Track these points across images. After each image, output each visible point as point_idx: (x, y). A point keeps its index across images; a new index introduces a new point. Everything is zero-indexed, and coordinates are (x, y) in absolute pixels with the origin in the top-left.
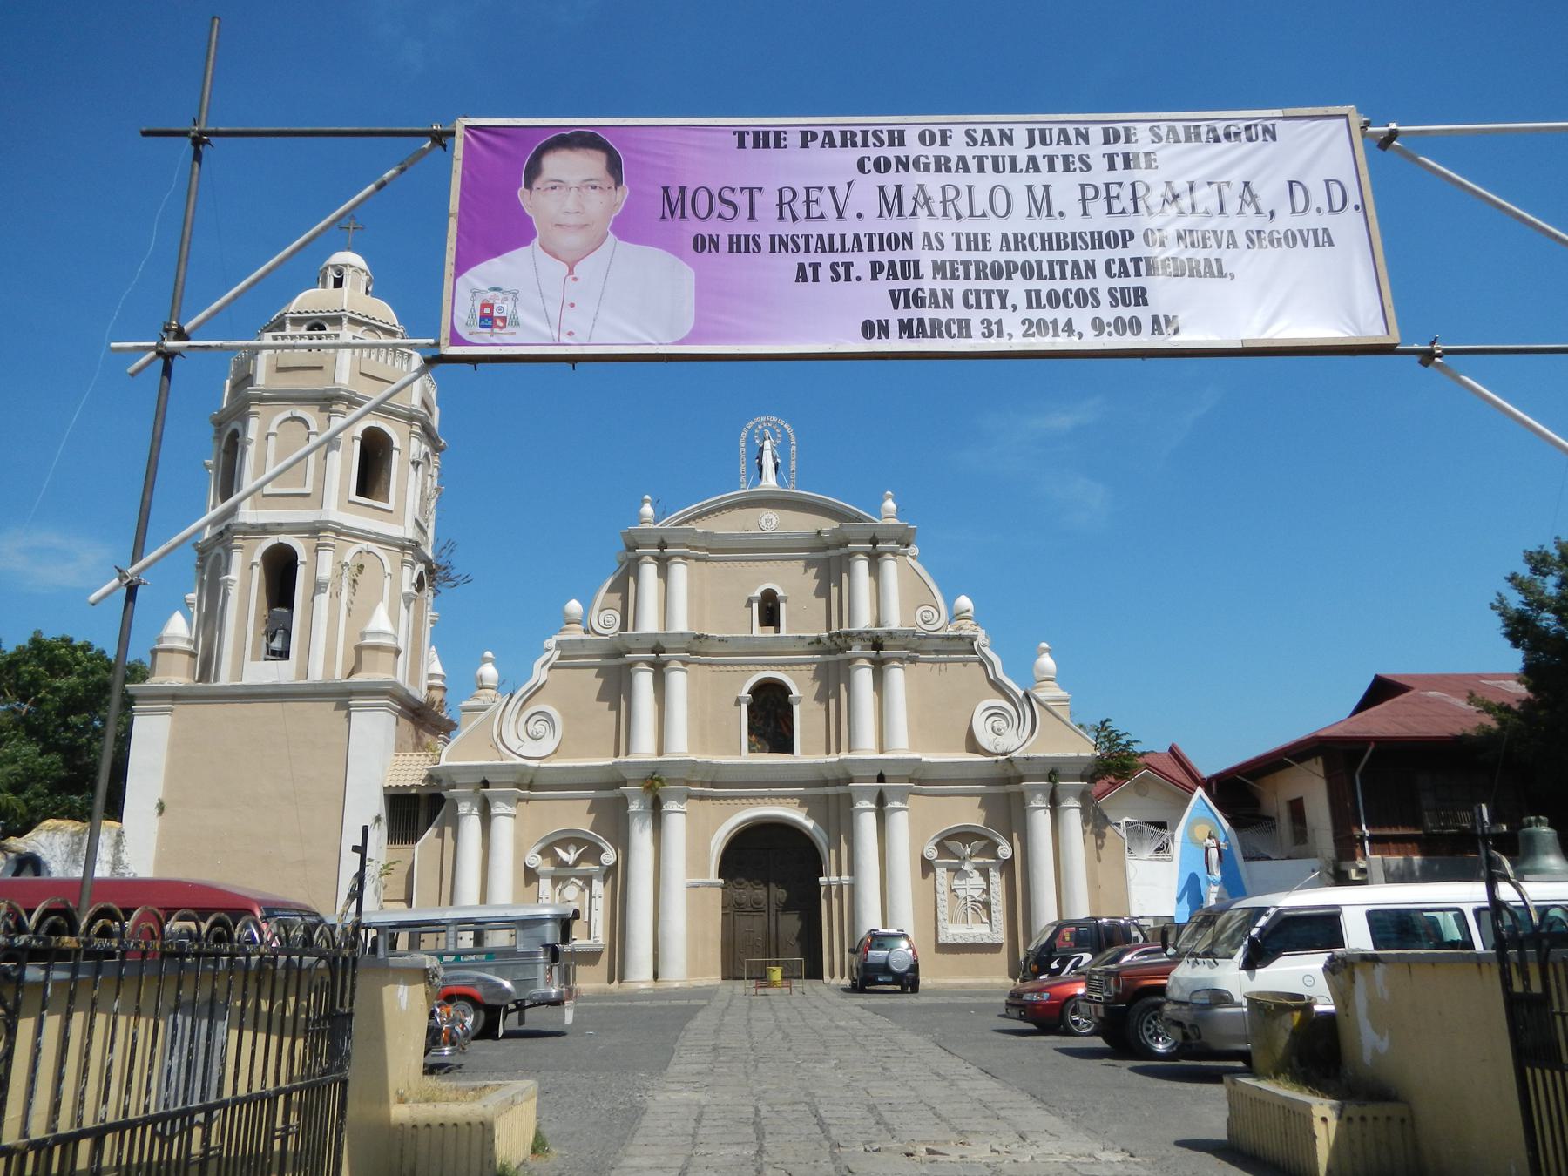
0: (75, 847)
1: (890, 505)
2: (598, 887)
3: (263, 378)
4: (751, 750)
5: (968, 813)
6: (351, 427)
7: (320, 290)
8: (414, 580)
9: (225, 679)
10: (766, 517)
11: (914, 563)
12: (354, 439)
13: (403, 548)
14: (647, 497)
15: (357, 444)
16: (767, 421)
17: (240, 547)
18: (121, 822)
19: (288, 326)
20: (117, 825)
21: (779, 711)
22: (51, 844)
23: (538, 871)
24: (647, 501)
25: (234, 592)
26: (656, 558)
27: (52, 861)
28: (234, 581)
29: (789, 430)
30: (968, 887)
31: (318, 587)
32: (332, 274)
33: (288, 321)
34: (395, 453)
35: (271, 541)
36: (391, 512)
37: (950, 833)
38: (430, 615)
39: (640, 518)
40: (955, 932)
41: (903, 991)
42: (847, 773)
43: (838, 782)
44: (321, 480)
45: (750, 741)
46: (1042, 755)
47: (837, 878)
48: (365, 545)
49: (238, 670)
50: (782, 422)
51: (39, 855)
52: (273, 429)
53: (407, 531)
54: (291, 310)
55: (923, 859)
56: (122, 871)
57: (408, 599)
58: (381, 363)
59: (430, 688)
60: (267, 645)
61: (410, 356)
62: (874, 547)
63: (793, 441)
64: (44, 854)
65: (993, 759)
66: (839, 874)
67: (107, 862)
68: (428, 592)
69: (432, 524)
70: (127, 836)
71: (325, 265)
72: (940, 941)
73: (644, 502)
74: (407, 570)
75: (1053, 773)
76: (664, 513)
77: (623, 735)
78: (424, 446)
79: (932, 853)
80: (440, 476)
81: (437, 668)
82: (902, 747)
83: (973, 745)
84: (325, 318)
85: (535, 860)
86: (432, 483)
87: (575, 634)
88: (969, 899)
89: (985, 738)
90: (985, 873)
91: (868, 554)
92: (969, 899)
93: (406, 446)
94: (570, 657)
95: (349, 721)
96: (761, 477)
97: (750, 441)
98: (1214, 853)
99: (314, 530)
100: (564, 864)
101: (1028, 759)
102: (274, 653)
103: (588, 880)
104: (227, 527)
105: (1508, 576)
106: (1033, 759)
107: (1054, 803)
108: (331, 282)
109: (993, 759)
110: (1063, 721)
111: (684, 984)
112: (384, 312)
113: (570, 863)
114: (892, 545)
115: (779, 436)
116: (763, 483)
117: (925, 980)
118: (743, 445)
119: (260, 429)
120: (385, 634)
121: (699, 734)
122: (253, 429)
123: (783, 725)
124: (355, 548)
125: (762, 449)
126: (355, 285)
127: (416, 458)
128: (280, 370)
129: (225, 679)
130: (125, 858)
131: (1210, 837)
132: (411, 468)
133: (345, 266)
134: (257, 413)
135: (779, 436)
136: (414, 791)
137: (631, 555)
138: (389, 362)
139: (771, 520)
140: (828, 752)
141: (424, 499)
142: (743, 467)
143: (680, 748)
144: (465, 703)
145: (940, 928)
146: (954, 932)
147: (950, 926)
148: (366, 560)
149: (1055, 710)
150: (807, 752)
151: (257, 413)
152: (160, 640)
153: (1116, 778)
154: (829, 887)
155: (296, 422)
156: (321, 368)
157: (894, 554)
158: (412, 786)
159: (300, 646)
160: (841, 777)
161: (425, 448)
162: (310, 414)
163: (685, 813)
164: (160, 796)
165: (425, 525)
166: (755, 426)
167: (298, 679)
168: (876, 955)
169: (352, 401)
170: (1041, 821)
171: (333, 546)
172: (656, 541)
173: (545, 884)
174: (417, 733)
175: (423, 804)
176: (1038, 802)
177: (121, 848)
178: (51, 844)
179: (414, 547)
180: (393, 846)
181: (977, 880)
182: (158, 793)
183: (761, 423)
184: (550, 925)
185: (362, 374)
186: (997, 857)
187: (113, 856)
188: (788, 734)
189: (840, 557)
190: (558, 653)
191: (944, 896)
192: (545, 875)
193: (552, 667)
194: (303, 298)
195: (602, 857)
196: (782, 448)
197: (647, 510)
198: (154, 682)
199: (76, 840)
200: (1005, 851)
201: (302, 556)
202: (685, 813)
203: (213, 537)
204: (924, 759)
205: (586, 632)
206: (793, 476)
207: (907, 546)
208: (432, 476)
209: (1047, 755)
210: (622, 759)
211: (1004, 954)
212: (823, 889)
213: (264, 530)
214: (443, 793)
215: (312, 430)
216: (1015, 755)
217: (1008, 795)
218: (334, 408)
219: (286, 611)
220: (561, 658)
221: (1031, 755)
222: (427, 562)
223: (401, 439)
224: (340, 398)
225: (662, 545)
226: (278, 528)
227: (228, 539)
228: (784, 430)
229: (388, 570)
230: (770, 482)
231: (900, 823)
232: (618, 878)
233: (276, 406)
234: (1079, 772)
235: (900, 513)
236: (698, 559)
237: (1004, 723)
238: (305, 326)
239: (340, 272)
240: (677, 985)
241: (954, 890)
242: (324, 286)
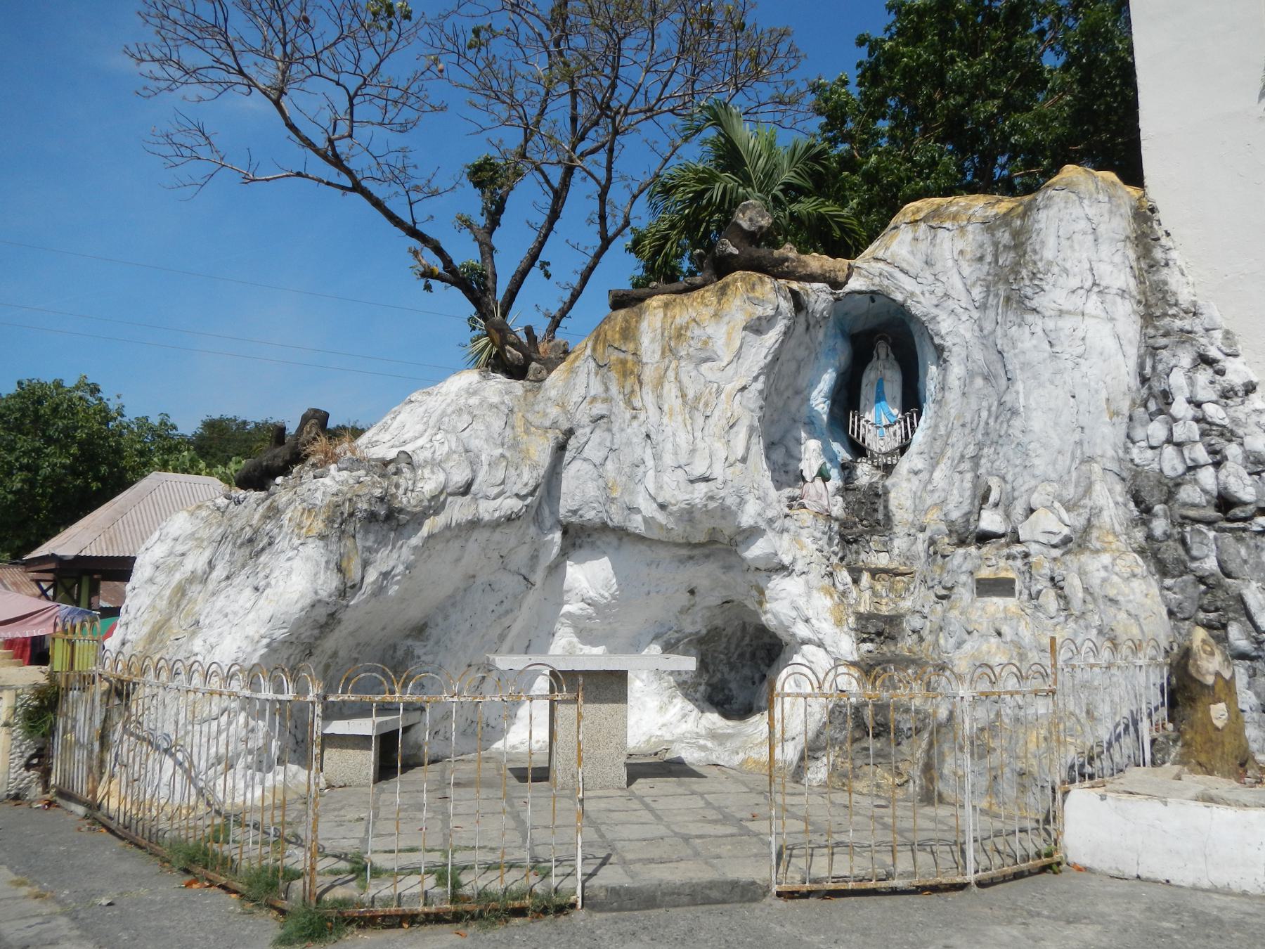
0: (1006, 259)
18: (1132, 174)
27: (942, 315)
51: (899, 297)
56: (1178, 324)
64: (906, 290)
67: (1123, 293)
70: (1167, 218)
130: (1182, 288)
177: (1158, 254)
199: (1005, 237)
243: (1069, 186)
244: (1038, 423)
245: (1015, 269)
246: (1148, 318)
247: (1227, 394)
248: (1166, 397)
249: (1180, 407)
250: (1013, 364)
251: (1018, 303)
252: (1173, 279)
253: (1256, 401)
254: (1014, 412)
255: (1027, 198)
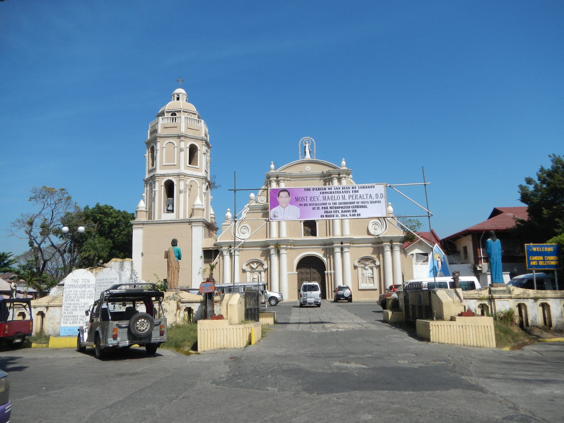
1: (344, 163)
2: (263, 273)
3: (160, 131)
4: (304, 235)
5: (368, 251)
6: (185, 145)
7: (172, 102)
8: (206, 188)
9: (156, 219)
10: (307, 167)
11: (351, 180)
12: (187, 148)
13: (202, 179)
14: (272, 162)
15: (188, 149)
16: (307, 138)
17: (158, 181)
18: (132, 258)
19: (166, 114)
20: (131, 259)
21: (312, 224)
22: (115, 265)
23: (246, 270)
24: (272, 163)
25: (157, 194)
26: (276, 181)
28: (157, 191)
29: (313, 141)
30: (367, 273)
31: (180, 192)
32: (176, 96)
33: (165, 113)
34: (199, 151)
35: (166, 179)
36: (198, 168)
37: (362, 258)
38: (210, 197)
39: (270, 169)
40: (364, 286)
41: (348, 302)
42: (332, 242)
43: (329, 244)
44: (179, 161)
45: (304, 233)
46: (388, 236)
47: (330, 271)
48: (192, 179)
49: (160, 216)
50: (311, 138)
52: (164, 146)
53: (203, 174)
54: (166, 109)
55: (354, 265)
57: (205, 194)
58: (194, 125)
59: (211, 218)
60: (167, 209)
61: (201, 121)
62: (339, 176)
63: (315, 144)
65: (374, 237)
66: (331, 270)
68: (209, 190)
69: (209, 171)
70: (134, 262)
71: (174, 93)
72: (359, 289)
73: (271, 164)
74: (204, 185)
75: (391, 241)
76: (278, 166)
77: (268, 231)
78: (206, 148)
79: (357, 264)
80: (210, 156)
81: (212, 212)
82: (348, 234)
83: (369, 234)
84: (176, 111)
85: (245, 267)
86: (209, 158)
87: (254, 204)
88: (367, 277)
89: (372, 231)
90: (372, 269)
91: (337, 178)
92: (367, 277)
93: (202, 148)
94: (252, 210)
95: (192, 229)
96: (305, 155)
97: (302, 144)
98: (440, 263)
99: (178, 175)
100: (253, 268)
101: (384, 237)
102: (168, 210)
103: (260, 272)
104: (154, 175)
105: (519, 185)
106: (385, 237)
107: (392, 248)
108: (176, 99)
109: (374, 237)
110: (394, 225)
111: (288, 301)
112: (192, 108)
113: (255, 268)
114: (344, 175)
115: (310, 143)
116: (306, 157)
117: (354, 299)
118: (300, 146)
119: (160, 146)
120: (200, 205)
121: (289, 232)
122: (159, 146)
123: (313, 228)
124: (190, 180)
125: (305, 147)
126: (183, 99)
127: (204, 152)
128: (165, 128)
129: (156, 219)
130: (134, 269)
131: (439, 258)
132: (203, 155)
133: (180, 93)
134: (159, 141)
135: (310, 143)
136: (211, 249)
137: (268, 180)
138: (195, 124)
139: (309, 168)
140: (327, 236)
141: (207, 163)
142: (300, 153)
143: (284, 235)
144: (223, 224)
145: (359, 285)
146: (363, 286)
147: (362, 284)
148: (193, 184)
149: (392, 222)
150: (321, 235)
151: (159, 141)
152: (138, 208)
153: (410, 242)
154: (328, 274)
155: (171, 143)
156: (176, 127)
157: (345, 178)
158: (210, 248)
159: (176, 209)
160: (330, 243)
161: (206, 148)
162: (175, 141)
163: (286, 254)
164: (142, 251)
165: (207, 171)
166: (303, 140)
167: (177, 218)
168: (341, 292)
169: (186, 137)
170: (388, 254)
171: (183, 180)
172: (276, 176)
173: (248, 274)
174: (209, 231)
175: (213, 252)
176: (387, 249)
178: (115, 265)
179: (206, 178)
180: (206, 264)
181: (370, 271)
182: (141, 251)
183: (305, 139)
184: (262, 286)
185: (188, 128)
186: (375, 265)
187: (131, 268)
188: (315, 230)
189: (329, 179)
190: (249, 209)
191: (361, 276)
192: (248, 271)
193: (247, 213)
194: (169, 104)
195: (264, 266)
196: (311, 146)
197: (272, 166)
198: (136, 220)
200: (378, 263)
201: (175, 183)
202: (286, 254)
203: (149, 177)
204: (354, 238)
205: (256, 203)
206: (315, 155)
207: (349, 175)
208: (208, 156)
209: (389, 236)
210: (268, 239)
211: (378, 291)
212: (326, 274)
213: (164, 175)
214: (219, 249)
215: (175, 146)
216: (380, 236)
217: (379, 247)
218: (181, 139)
219: (172, 199)
220: (249, 210)
221: (385, 236)
222: (209, 182)
223: (200, 147)
224: (182, 136)
225: (277, 177)
226: (168, 175)
227: (154, 178)
228: (312, 141)
229: (199, 186)
230: (308, 156)
231: (347, 256)
232: (268, 271)
233: (165, 139)
234: (399, 241)
235: (346, 166)
236: (287, 180)
237: (377, 226)
238: (171, 113)
239: (178, 95)
240: (286, 301)
241: (363, 274)
242: (174, 100)
243: (127, 261)
244: (123, 280)
245: (122, 267)
246: (132, 271)
247: (136, 278)
248: (132, 278)
249: (133, 279)
250: (122, 275)
251: (122, 270)
252: (133, 268)
253: (138, 278)
254: (121, 279)
255: (123, 260)
